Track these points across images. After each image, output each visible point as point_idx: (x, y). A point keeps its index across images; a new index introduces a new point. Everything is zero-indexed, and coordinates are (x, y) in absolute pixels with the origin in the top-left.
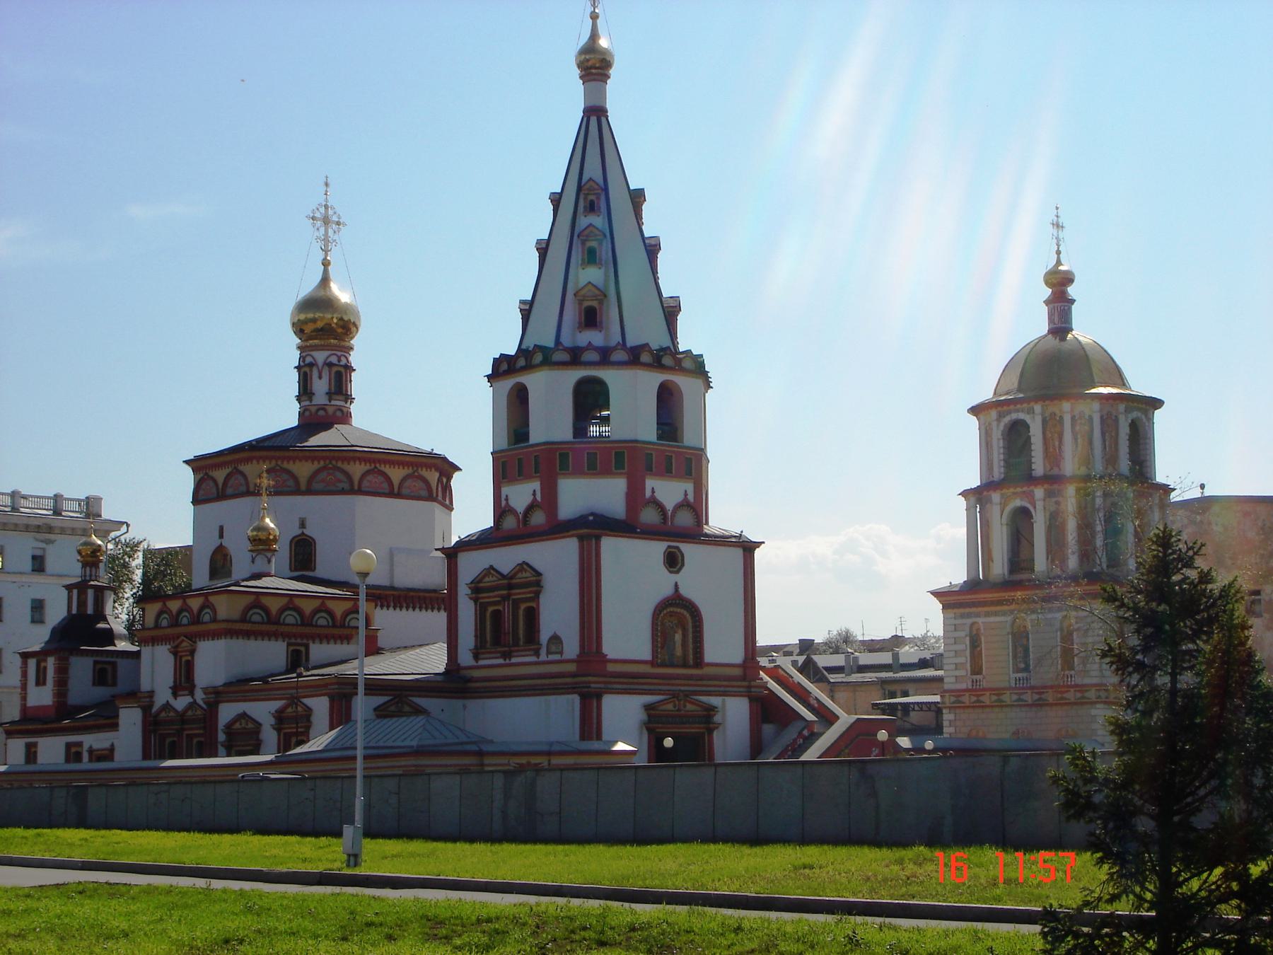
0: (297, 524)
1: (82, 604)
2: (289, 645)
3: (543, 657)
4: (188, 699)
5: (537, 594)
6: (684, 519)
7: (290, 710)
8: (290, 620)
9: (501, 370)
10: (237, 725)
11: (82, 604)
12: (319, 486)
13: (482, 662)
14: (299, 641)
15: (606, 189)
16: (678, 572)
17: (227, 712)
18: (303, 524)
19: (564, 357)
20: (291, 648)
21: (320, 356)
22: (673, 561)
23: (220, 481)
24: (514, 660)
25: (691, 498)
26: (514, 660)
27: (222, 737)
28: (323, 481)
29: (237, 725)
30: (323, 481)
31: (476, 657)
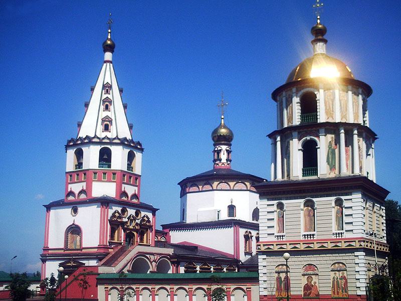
9: (72, 144)
15: (111, 87)
19: (97, 140)
25: (137, 193)
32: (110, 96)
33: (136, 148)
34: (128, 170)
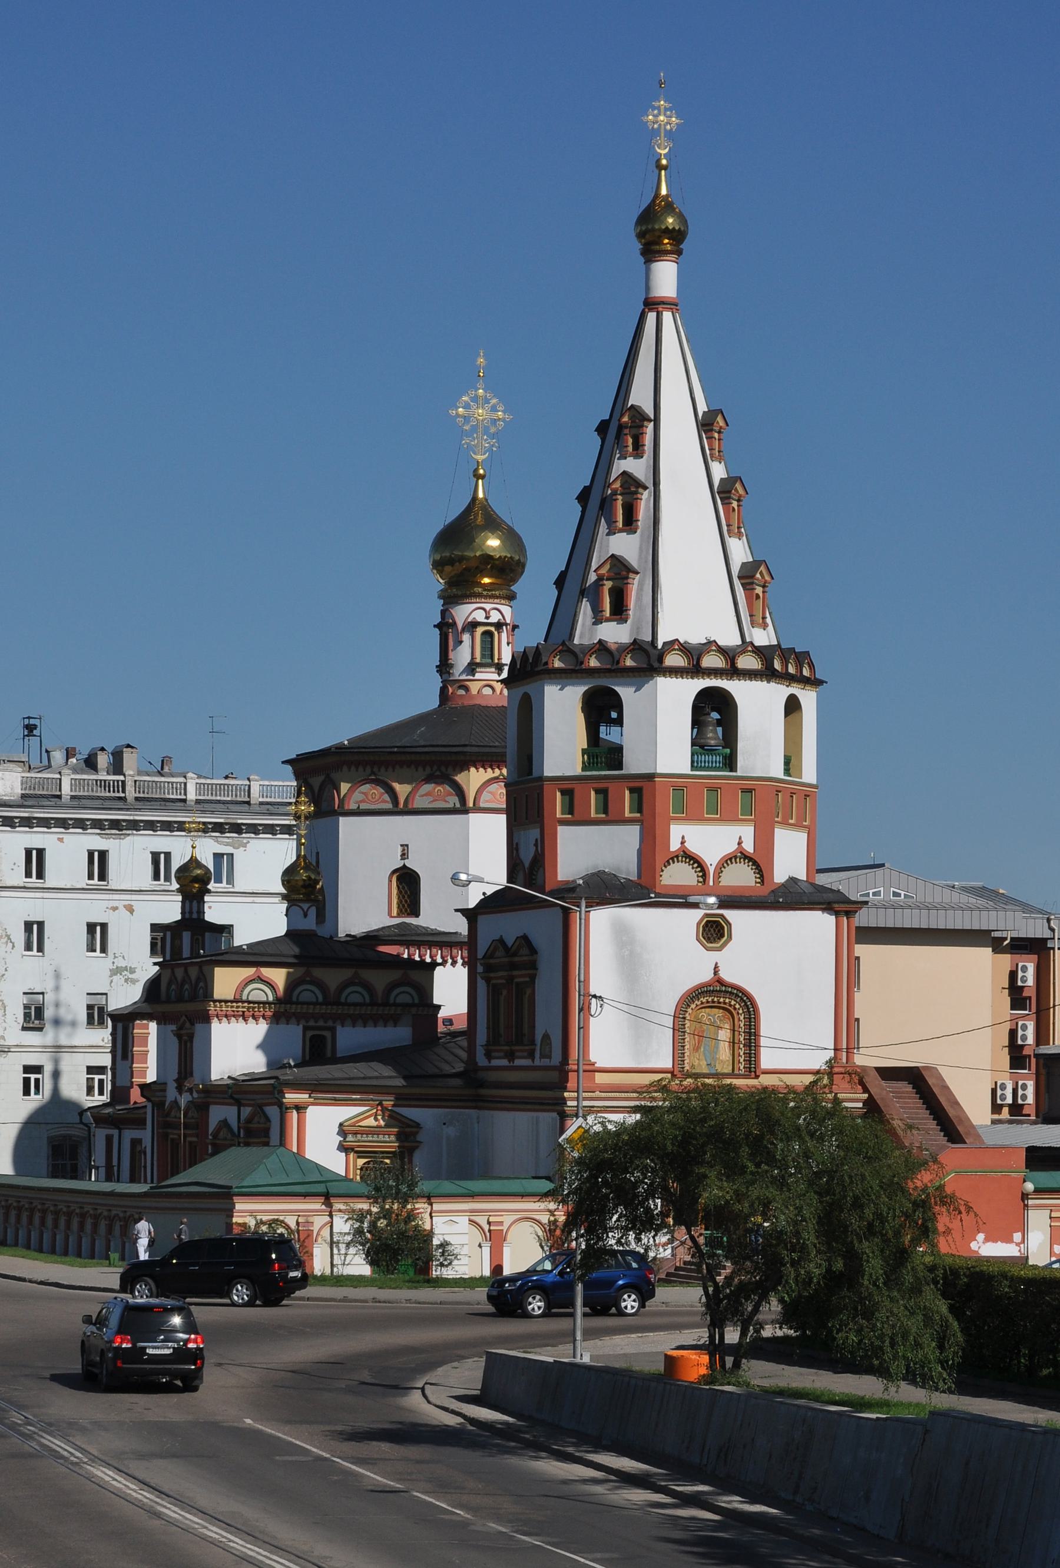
2: (306, 1029)
3: (537, 1062)
5: (533, 978)
6: (741, 877)
13: (495, 1062)
14: (321, 1023)
16: (720, 949)
18: (404, 856)
22: (714, 932)
24: (518, 1062)
25: (749, 847)
26: (518, 1062)
28: (428, 794)
30: (428, 794)
31: (489, 1056)
32: (637, 467)
33: (733, 672)
34: (693, 768)
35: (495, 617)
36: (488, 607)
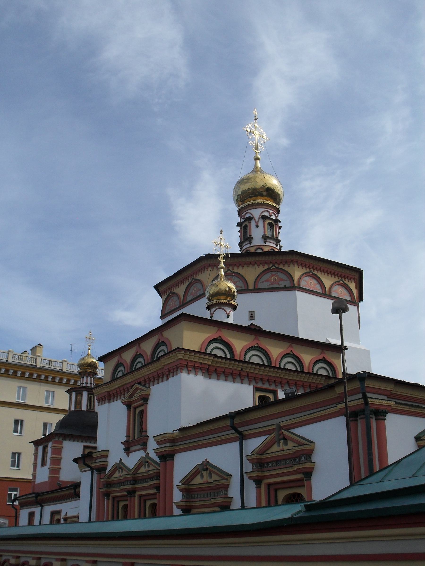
0: (247, 316)
1: (78, 403)
4: (141, 454)
7: (275, 448)
8: (256, 360)
10: (198, 480)
11: (78, 403)
12: (266, 285)
14: (266, 386)
17: (184, 464)
18: (252, 318)
20: (258, 394)
21: (256, 213)
23: (182, 295)
27: (178, 496)
28: (267, 281)
29: (198, 480)
30: (267, 281)
35: (273, 217)
36: (271, 211)
